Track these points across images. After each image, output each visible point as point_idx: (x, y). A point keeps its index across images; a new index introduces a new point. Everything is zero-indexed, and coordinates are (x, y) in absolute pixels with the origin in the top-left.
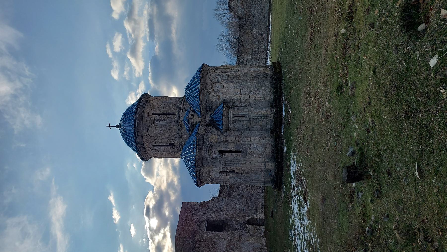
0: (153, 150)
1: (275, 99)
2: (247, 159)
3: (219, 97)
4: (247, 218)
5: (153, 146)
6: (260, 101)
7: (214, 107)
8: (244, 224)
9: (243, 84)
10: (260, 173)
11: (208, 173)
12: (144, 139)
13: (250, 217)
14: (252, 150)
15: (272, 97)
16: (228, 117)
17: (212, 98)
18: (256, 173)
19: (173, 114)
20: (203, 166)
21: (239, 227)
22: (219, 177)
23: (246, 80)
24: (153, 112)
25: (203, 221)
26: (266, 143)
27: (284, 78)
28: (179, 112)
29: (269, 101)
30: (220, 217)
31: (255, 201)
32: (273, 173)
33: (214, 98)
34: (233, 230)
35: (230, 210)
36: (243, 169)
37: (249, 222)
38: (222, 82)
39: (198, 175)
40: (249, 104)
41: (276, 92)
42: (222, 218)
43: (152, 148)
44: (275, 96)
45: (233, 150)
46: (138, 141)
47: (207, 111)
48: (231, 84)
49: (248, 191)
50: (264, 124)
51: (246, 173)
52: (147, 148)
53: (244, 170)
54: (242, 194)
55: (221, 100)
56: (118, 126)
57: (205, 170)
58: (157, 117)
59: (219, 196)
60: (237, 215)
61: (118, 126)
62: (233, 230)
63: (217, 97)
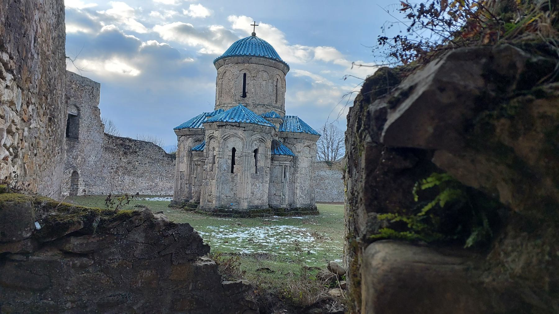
0: (238, 72)
1: (296, 209)
2: (250, 179)
3: (299, 152)
4: (79, 172)
5: (245, 75)
6: (294, 194)
7: (289, 146)
8: (74, 167)
10: (232, 193)
11: (235, 135)
12: (255, 66)
13: (80, 176)
14: (258, 185)
15: (298, 206)
18: (232, 189)
19: (276, 102)
21: (71, 160)
22: (227, 147)
23: (310, 180)
24: (279, 80)
25: (79, 110)
26: (263, 200)
27: (216, 218)
28: (278, 108)
30: (83, 134)
31: (98, 183)
32: (234, 208)
33: (299, 147)
34: (68, 151)
35: (88, 147)
36: (239, 174)
37: (75, 173)
38: (311, 156)
39: (234, 124)
40: (293, 182)
41: (303, 210)
42: (80, 136)
43: (243, 72)
44: (300, 208)
45: (258, 164)
46: (254, 59)
47: (284, 139)
50: (277, 198)
51: (233, 178)
52: (242, 66)
53: (236, 175)
54: (106, 166)
55: (296, 154)
56: (254, 34)
57: (240, 132)
61: (254, 34)
62: (68, 151)
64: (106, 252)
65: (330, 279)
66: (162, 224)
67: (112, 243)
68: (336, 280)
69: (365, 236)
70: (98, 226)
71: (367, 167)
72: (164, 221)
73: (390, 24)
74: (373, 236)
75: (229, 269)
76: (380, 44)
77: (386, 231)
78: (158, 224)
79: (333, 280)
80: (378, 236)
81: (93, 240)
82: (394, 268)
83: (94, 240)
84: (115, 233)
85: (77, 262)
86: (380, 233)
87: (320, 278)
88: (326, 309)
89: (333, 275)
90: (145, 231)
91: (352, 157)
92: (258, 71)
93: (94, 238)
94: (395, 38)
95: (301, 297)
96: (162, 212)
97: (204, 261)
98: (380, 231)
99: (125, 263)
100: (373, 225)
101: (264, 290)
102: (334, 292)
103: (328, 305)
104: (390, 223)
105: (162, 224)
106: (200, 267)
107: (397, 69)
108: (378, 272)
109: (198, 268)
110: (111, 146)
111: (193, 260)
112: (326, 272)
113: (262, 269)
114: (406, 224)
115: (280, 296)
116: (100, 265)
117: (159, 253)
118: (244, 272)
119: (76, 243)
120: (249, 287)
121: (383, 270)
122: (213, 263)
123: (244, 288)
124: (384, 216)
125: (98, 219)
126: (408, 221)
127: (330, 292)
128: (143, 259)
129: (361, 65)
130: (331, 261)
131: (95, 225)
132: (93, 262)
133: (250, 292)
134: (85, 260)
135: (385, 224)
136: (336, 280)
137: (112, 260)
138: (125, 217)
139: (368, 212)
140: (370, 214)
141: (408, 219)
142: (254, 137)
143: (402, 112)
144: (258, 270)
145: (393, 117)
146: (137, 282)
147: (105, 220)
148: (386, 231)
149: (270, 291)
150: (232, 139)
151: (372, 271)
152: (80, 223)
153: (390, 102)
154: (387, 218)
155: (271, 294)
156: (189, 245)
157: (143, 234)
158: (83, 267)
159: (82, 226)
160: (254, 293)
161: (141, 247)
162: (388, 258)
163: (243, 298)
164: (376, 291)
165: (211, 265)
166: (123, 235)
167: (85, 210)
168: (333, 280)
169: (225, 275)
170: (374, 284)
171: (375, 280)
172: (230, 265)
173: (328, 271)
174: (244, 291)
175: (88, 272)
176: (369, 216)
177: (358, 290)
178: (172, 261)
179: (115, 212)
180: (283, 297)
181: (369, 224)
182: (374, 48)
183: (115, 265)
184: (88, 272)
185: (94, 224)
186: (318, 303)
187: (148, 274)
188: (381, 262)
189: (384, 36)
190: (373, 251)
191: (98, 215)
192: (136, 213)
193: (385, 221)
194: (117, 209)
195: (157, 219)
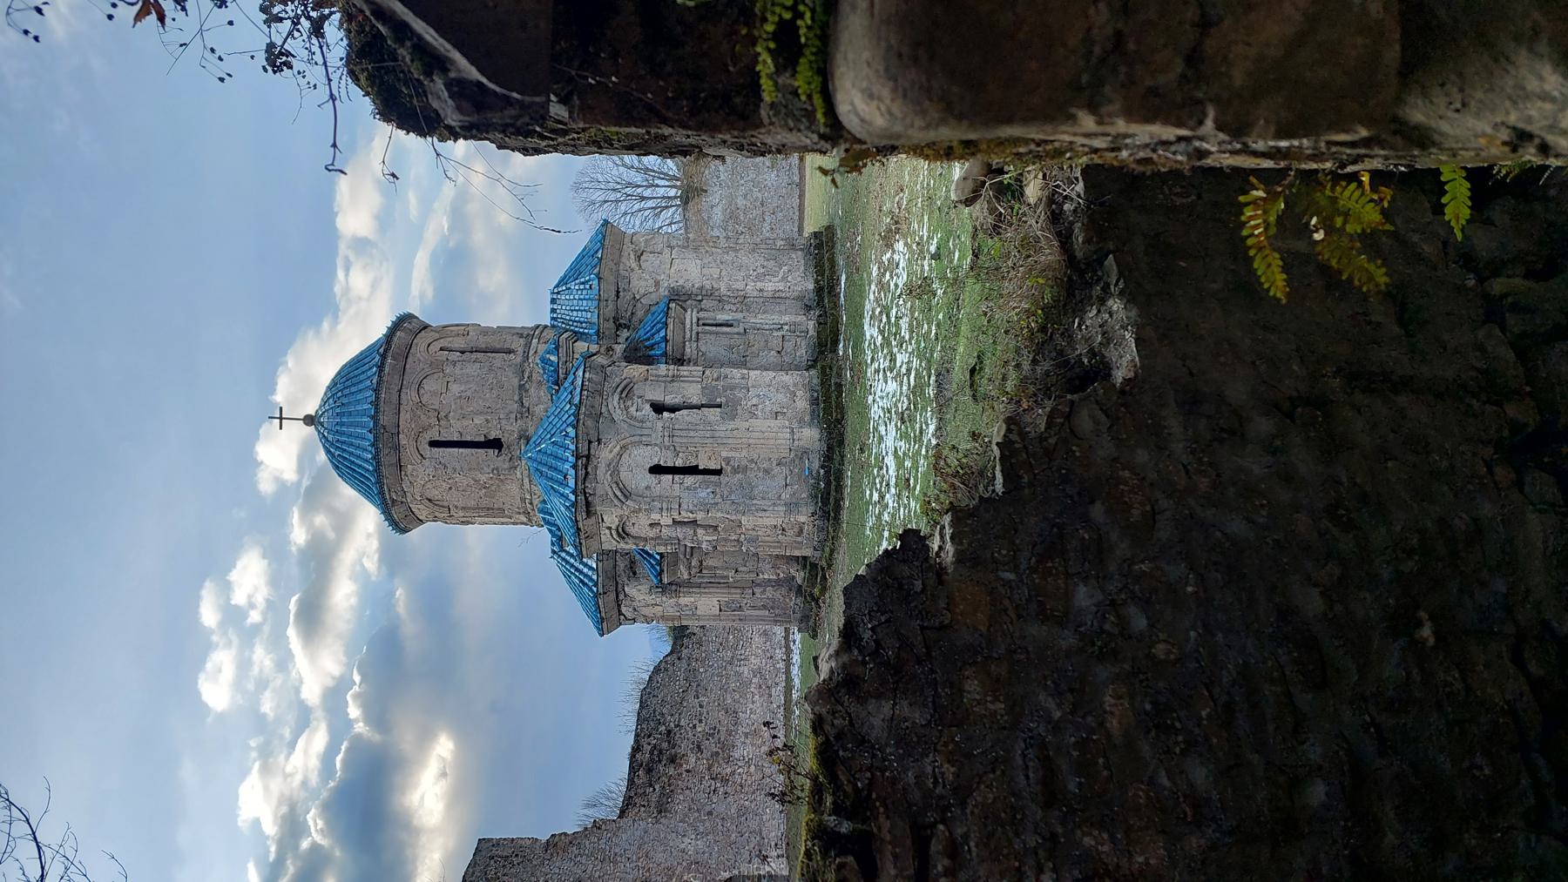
0: (426, 462)
1: (819, 290)
2: (738, 423)
3: (657, 284)
5: (434, 444)
6: (776, 298)
7: (640, 313)
9: (729, 258)
10: (777, 470)
11: (615, 472)
12: (405, 417)
13: (736, 872)
14: (755, 401)
15: (811, 286)
16: (683, 324)
17: (634, 282)
18: (766, 471)
19: (510, 352)
20: (599, 441)
22: (648, 488)
26: (795, 385)
27: (845, 515)
29: (800, 298)
31: (754, 825)
32: (816, 465)
35: (660, 857)
36: (724, 454)
38: (667, 250)
39: (582, 473)
40: (743, 300)
44: (817, 282)
45: (695, 400)
46: (385, 419)
47: (619, 327)
48: (692, 255)
49: (730, 799)
50: (789, 346)
51: (735, 471)
53: (728, 460)
54: (708, 808)
55: (663, 292)
56: (309, 420)
57: (604, 455)
58: (455, 356)
59: (622, 814)
60: (689, 869)
61: (309, 420)
63: (651, 282)
64: (916, 796)
65: (999, 201)
66: (845, 658)
67: (893, 781)
68: (1001, 182)
69: (822, 137)
70: (848, 819)
71: (642, 123)
72: (837, 653)
73: (208, 54)
74: (819, 116)
75: (969, 476)
76: (290, 67)
77: (803, 80)
78: (844, 666)
79: (1001, 190)
80: (818, 100)
81: (885, 830)
82: (887, 70)
83: (884, 827)
84: (868, 775)
85: (941, 864)
86: (810, 97)
87: (996, 229)
88: (1075, 211)
89: (987, 192)
90: (862, 701)
91: (637, 145)
92: (421, 405)
93: (879, 829)
94: (268, 22)
95: (1041, 281)
96: (815, 659)
97: (943, 546)
98: (803, 98)
99: (946, 745)
100: (794, 113)
101: (1023, 381)
102: (1033, 191)
103: (1066, 207)
104: (785, 69)
105: (845, 658)
106: (958, 553)
107: (349, 31)
108: (896, 110)
109: (960, 558)
110: (654, 798)
111: (940, 571)
112: (979, 210)
113: (972, 385)
114: (782, 23)
115: (1040, 337)
116: (948, 808)
117: (919, 662)
118: (974, 436)
119: (893, 872)
120: (1011, 422)
121: (893, 100)
122: (947, 519)
123: (1014, 437)
124: (766, 83)
125: (831, 820)
126: (772, 18)
127: (1032, 201)
128: (934, 702)
129: (334, 145)
130: (953, 197)
131: (845, 827)
132: (941, 827)
133: (1027, 418)
134: (935, 847)
135: (783, 79)
136: (1001, 182)
137: (936, 779)
138: (826, 755)
139: (760, 125)
140: (766, 121)
141: (764, 20)
142: (618, 415)
143: (448, 46)
144: (974, 397)
145: (468, 70)
146: (994, 714)
147: (834, 803)
148: (803, 80)
149: (1026, 366)
150: (624, 475)
151: (898, 128)
152: (841, 867)
153: (428, 74)
154: (770, 77)
155: (1034, 362)
156: (901, 586)
157: (872, 705)
158: (954, 850)
159: (850, 859)
160: (1030, 409)
161: (904, 708)
162: (864, 84)
163: (1042, 438)
164: (943, 122)
165: (953, 524)
166: (874, 756)
167: (808, 854)
168: (1001, 190)
169: (981, 488)
170: (927, 127)
171: (918, 122)
172: (956, 475)
173: (977, 206)
174: (1023, 435)
175: (966, 837)
176: (772, 124)
177: (984, 147)
178: (942, 627)
179: (815, 779)
180: (1043, 329)
181: (791, 124)
182: (303, 82)
183: (949, 771)
184: (966, 837)
185: (843, 830)
186: (1059, 234)
187: (973, 687)
188: (875, 103)
189: (263, 55)
190: (856, 120)
191: (820, 823)
192: (818, 725)
193: (780, 81)
194: (806, 776)
195: (832, 672)
